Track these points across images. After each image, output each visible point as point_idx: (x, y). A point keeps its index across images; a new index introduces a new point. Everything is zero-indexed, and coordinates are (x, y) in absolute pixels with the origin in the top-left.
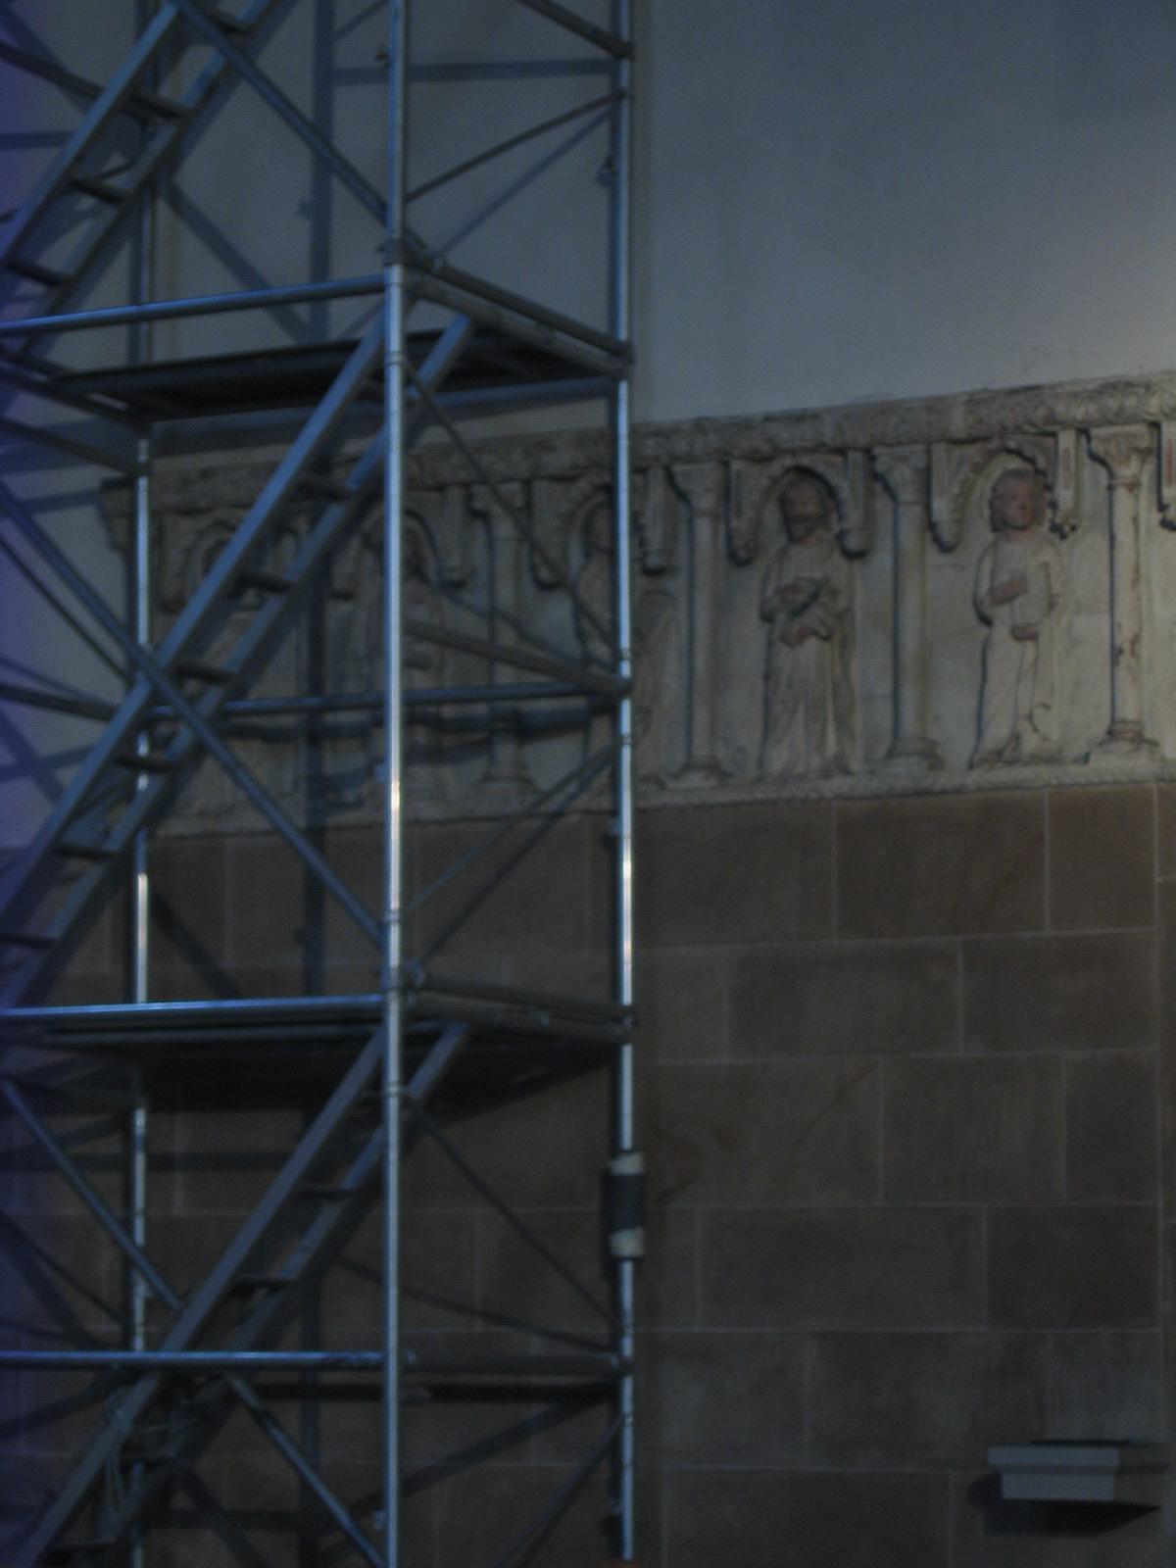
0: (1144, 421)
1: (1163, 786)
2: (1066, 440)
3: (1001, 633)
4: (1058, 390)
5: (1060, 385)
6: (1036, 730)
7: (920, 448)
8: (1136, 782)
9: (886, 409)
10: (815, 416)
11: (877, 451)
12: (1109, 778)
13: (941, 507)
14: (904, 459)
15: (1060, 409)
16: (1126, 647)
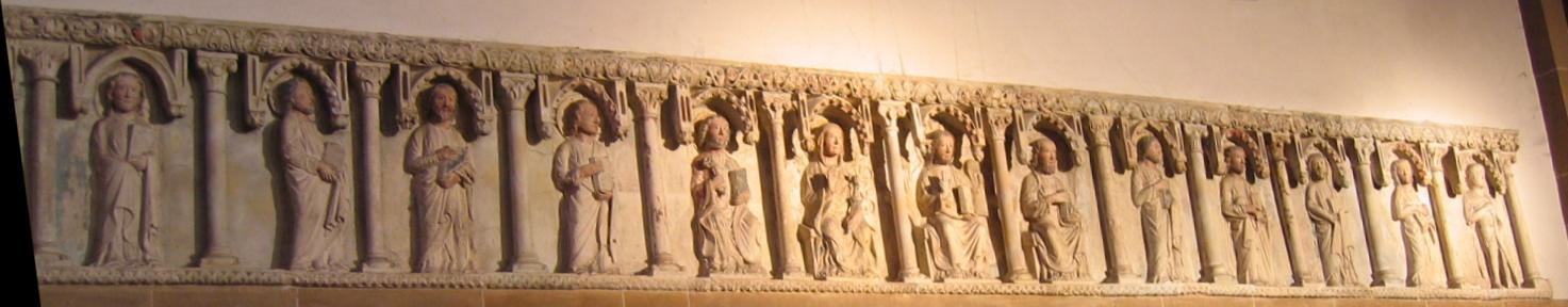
0: (670, 82)
1: (694, 293)
2: (621, 87)
3: (585, 194)
4: (622, 56)
5: (624, 53)
6: (610, 254)
7: (534, 76)
8: (679, 290)
9: (512, 49)
10: (468, 45)
11: (504, 74)
12: (664, 287)
13: (546, 114)
14: (522, 83)
15: (625, 67)
16: (663, 211)
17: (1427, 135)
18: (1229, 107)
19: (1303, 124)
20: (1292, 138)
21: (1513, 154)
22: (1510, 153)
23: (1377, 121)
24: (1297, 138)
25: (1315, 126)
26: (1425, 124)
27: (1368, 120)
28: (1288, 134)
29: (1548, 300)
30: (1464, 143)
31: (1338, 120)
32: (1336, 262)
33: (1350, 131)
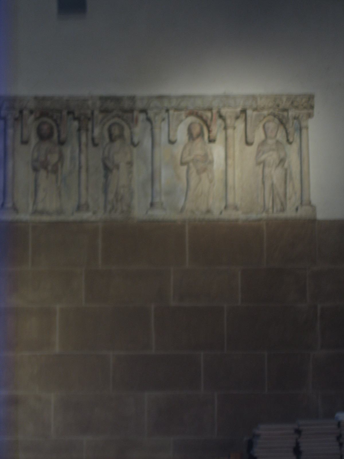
17: (215, 104)
18: (36, 98)
19: (98, 103)
20: (92, 113)
21: (310, 111)
22: (305, 111)
23: (169, 98)
24: (96, 113)
25: (110, 105)
26: (215, 97)
27: (161, 98)
28: (89, 112)
29: (313, 221)
30: (254, 106)
31: (133, 99)
32: (111, 197)
33: (139, 105)
